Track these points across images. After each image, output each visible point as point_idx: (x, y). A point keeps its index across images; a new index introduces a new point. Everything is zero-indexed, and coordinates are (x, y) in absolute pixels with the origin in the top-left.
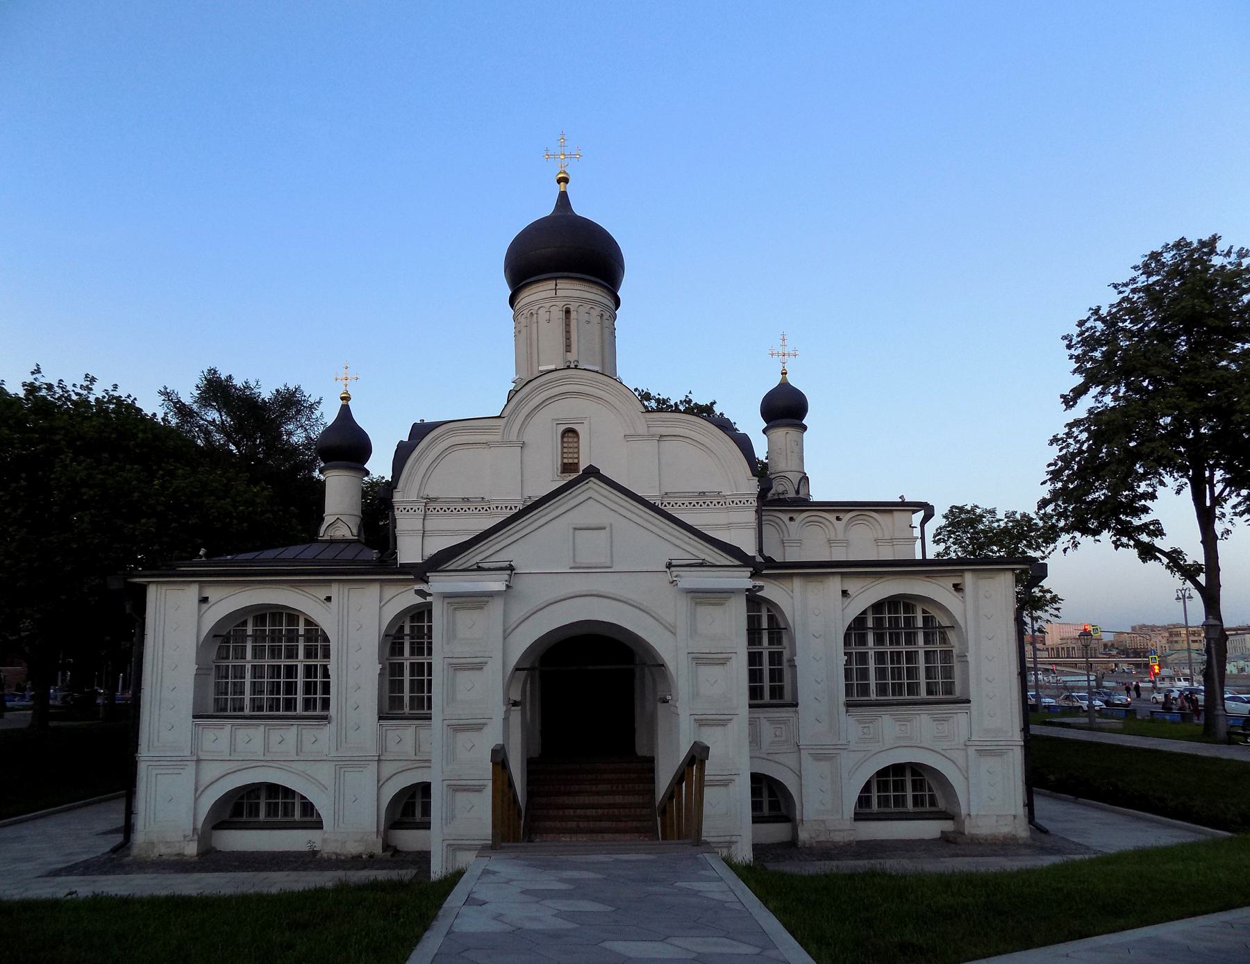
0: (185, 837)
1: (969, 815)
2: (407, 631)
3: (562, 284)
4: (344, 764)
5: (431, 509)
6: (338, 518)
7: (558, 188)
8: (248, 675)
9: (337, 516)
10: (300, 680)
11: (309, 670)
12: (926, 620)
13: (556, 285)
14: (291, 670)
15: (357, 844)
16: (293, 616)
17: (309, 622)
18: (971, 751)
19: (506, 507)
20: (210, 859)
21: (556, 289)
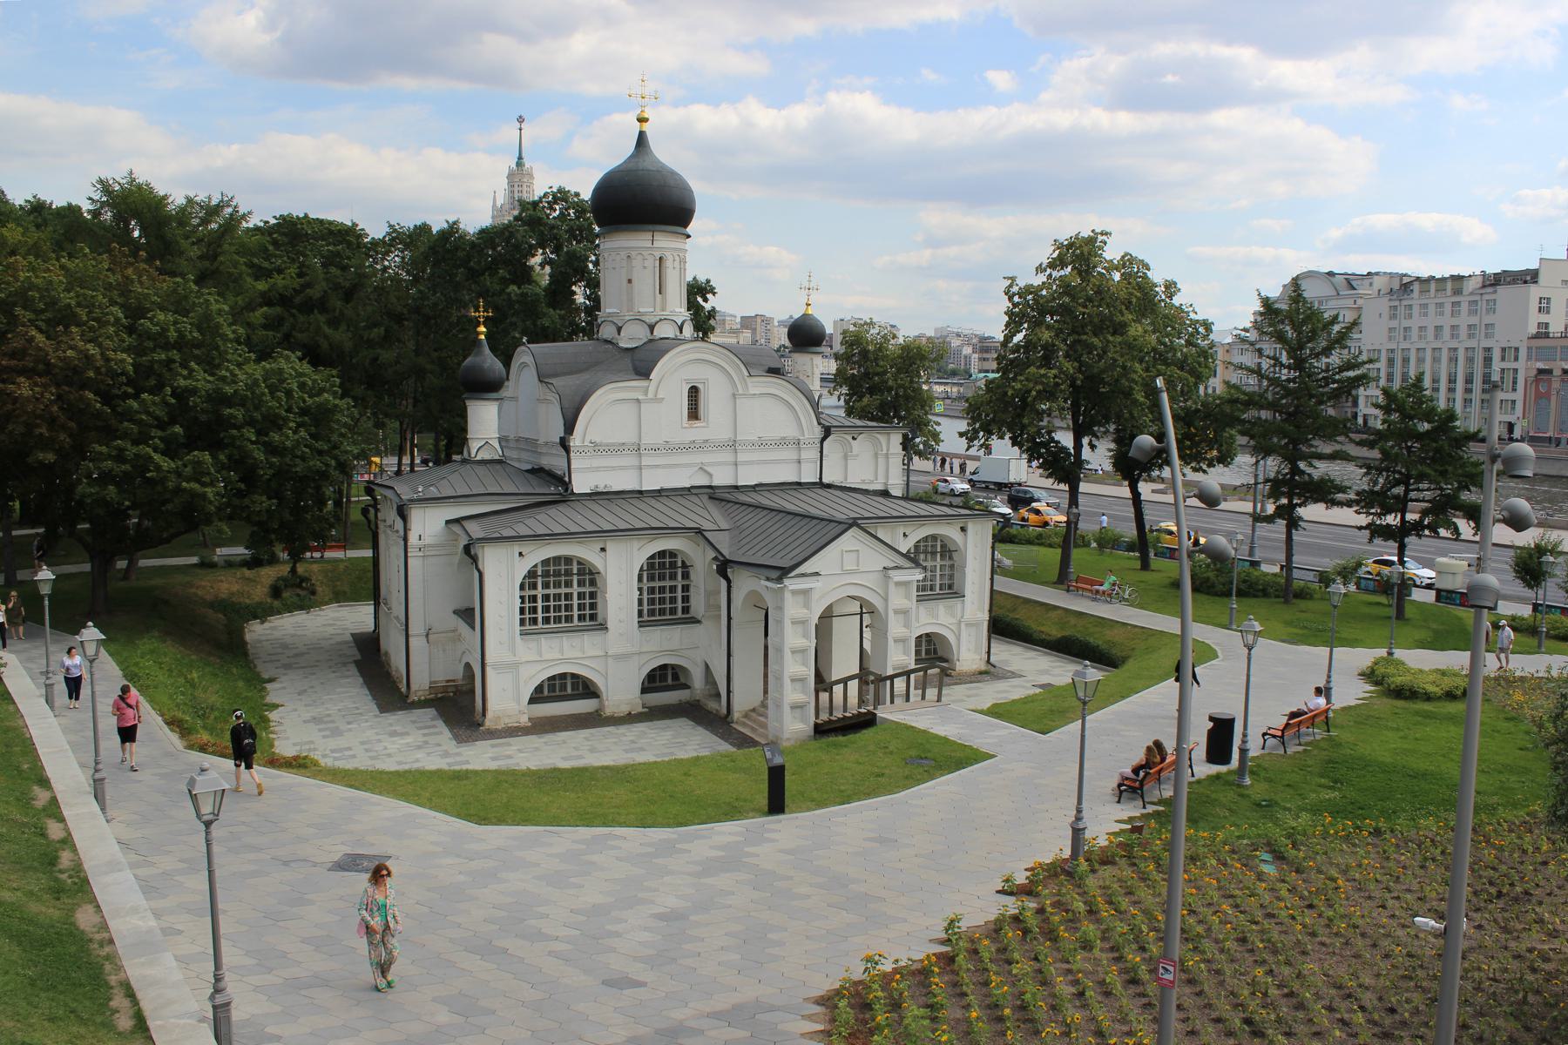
2: (645, 568)
3: (658, 236)
7: (637, 127)
8: (540, 600)
10: (575, 602)
11: (581, 596)
12: (942, 546)
14: (568, 596)
16: (568, 560)
17: (579, 563)
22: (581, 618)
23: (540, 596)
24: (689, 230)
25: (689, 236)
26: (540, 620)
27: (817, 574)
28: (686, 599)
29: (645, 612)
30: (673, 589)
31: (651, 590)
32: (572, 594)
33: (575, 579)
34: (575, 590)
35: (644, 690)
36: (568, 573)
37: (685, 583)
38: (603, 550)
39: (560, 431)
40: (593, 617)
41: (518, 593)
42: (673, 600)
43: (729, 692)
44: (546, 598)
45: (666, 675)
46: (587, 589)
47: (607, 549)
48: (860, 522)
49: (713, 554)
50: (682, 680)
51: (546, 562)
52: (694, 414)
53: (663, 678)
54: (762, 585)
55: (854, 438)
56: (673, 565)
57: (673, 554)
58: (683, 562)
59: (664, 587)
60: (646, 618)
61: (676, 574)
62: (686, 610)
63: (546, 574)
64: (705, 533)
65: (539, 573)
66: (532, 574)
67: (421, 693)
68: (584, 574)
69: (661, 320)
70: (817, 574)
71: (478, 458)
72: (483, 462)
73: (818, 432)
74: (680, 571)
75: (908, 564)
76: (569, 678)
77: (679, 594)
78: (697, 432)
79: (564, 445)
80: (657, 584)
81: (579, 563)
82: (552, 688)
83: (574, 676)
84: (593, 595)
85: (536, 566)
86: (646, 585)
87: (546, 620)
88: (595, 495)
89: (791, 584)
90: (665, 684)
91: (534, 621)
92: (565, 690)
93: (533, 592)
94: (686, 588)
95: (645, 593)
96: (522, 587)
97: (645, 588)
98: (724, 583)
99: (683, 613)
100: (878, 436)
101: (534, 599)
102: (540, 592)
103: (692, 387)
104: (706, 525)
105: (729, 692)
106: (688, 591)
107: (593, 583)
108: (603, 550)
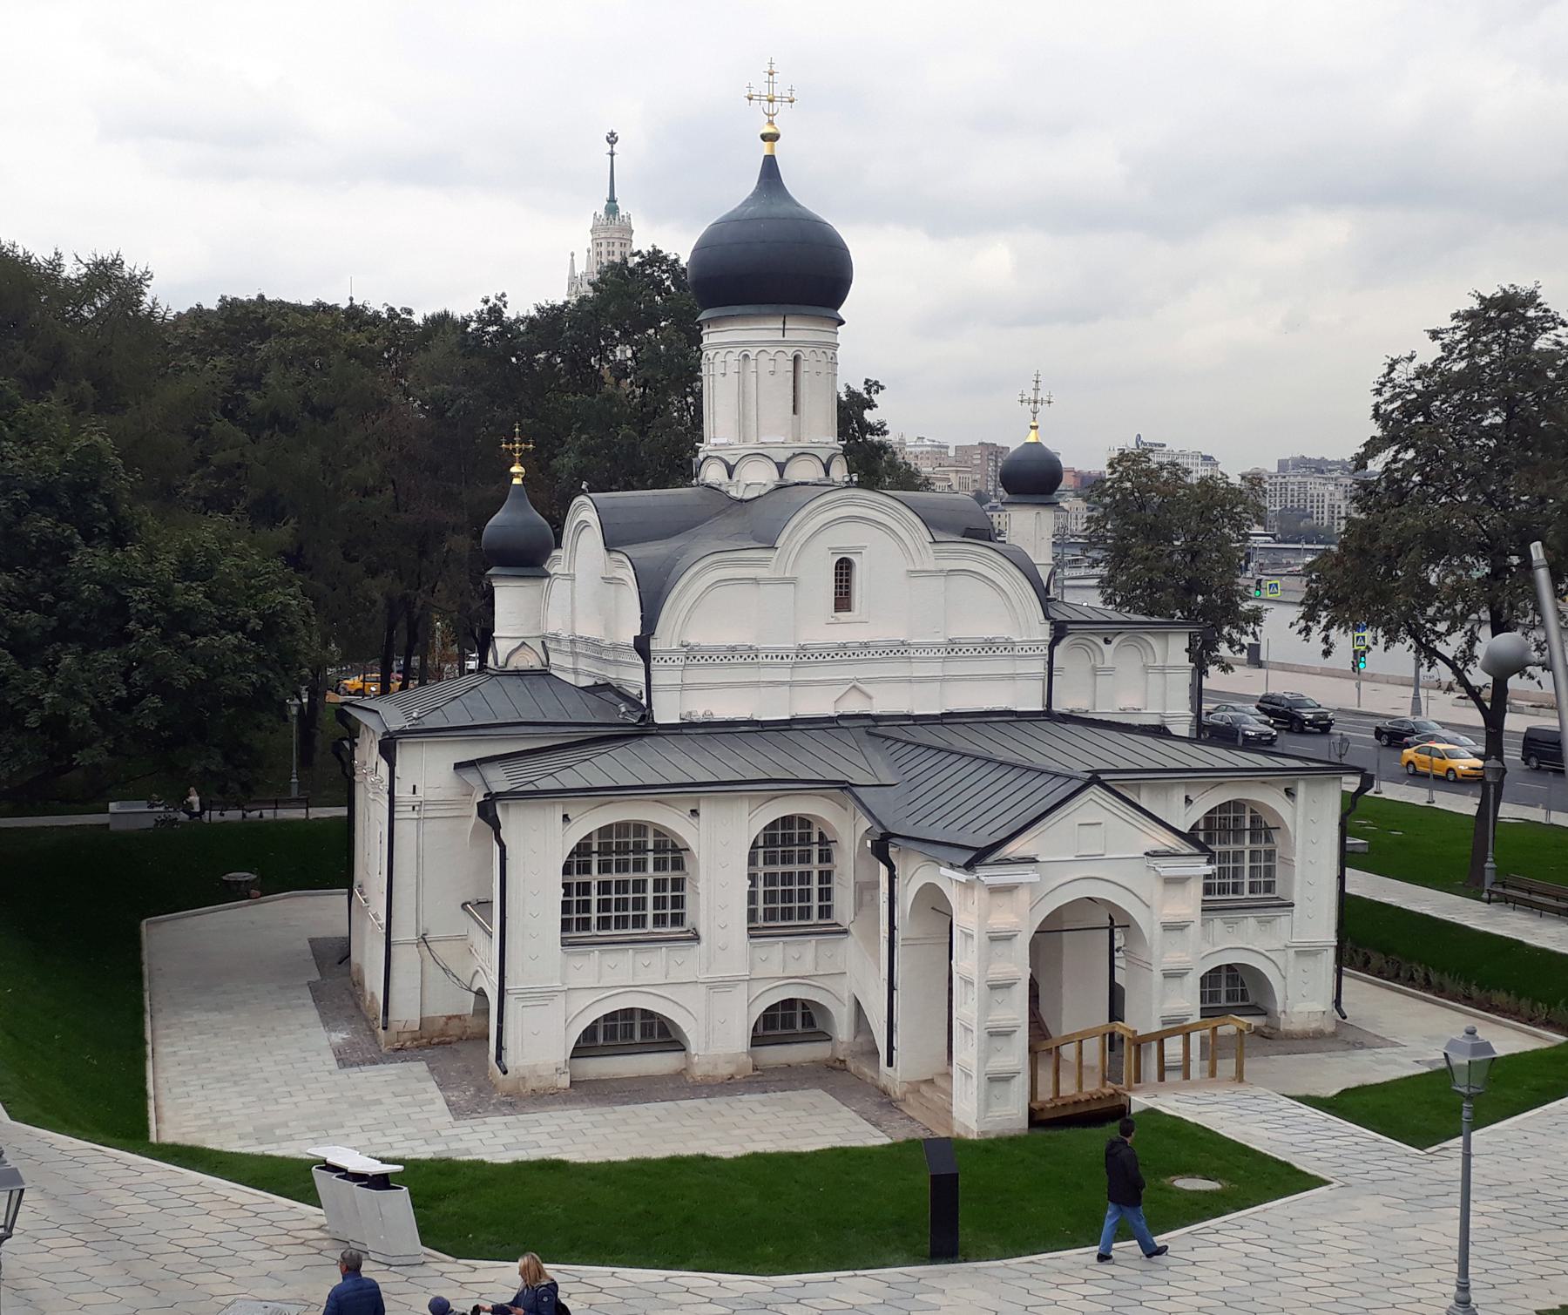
0: (557, 1070)
1: (1284, 1012)
2: (761, 843)
4: (719, 986)
5: (691, 657)
6: (524, 643)
8: (594, 891)
9: (522, 640)
11: (659, 885)
13: (784, 323)
14: (640, 886)
15: (728, 1065)
16: (641, 828)
17: (657, 833)
18: (1291, 952)
19: (777, 656)
20: (585, 1091)
21: (784, 329)
22: (659, 920)
23: (595, 884)
24: (842, 312)
25: (841, 322)
26: (594, 921)
27: (1033, 861)
28: (825, 894)
29: (761, 912)
30: (805, 877)
31: (770, 879)
32: (645, 881)
33: (651, 857)
34: (650, 875)
35: (757, 1040)
36: (640, 848)
37: (825, 867)
38: (694, 812)
39: (631, 628)
40: (678, 920)
41: (558, 878)
42: (805, 895)
43: (890, 1048)
44: (604, 887)
45: (793, 1017)
46: (669, 874)
47: (702, 812)
48: (1103, 777)
49: (866, 824)
50: (819, 1026)
51: (605, 831)
52: (843, 600)
53: (788, 1023)
54: (948, 878)
55: (1107, 641)
56: (805, 839)
57: (805, 822)
58: (821, 835)
59: (791, 874)
60: (761, 923)
61: (809, 852)
62: (825, 912)
63: (605, 849)
64: (859, 791)
65: (595, 848)
66: (582, 849)
67: (406, 1036)
68: (666, 851)
69: (795, 455)
70: (1033, 861)
71: (510, 668)
72: (518, 673)
73: (1043, 632)
74: (815, 849)
75: (1187, 849)
76: (638, 1017)
77: (815, 886)
78: (848, 630)
79: (642, 646)
80: (779, 869)
81: (657, 833)
82: (610, 1033)
83: (646, 1014)
84: (678, 884)
85: (589, 836)
86: (762, 869)
87: (604, 923)
88: (686, 729)
89: (988, 875)
90: (794, 1031)
91: (585, 924)
92: (632, 1037)
93: (584, 878)
94: (826, 877)
95: (761, 883)
96: (567, 870)
97: (761, 875)
98: (883, 869)
99: (820, 917)
100: (1148, 638)
101: (585, 888)
102: (595, 877)
103: (841, 561)
104: (858, 777)
105: (890, 1048)
106: (829, 881)
107: (678, 865)
108: (694, 812)
